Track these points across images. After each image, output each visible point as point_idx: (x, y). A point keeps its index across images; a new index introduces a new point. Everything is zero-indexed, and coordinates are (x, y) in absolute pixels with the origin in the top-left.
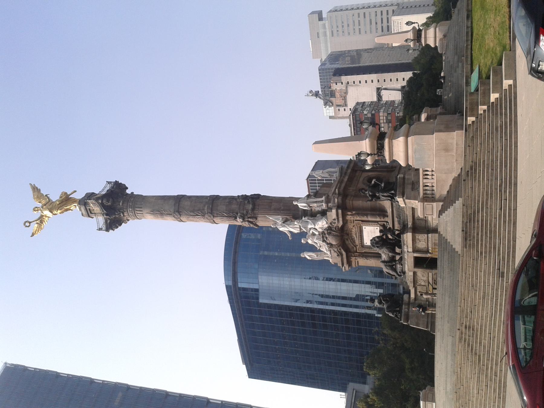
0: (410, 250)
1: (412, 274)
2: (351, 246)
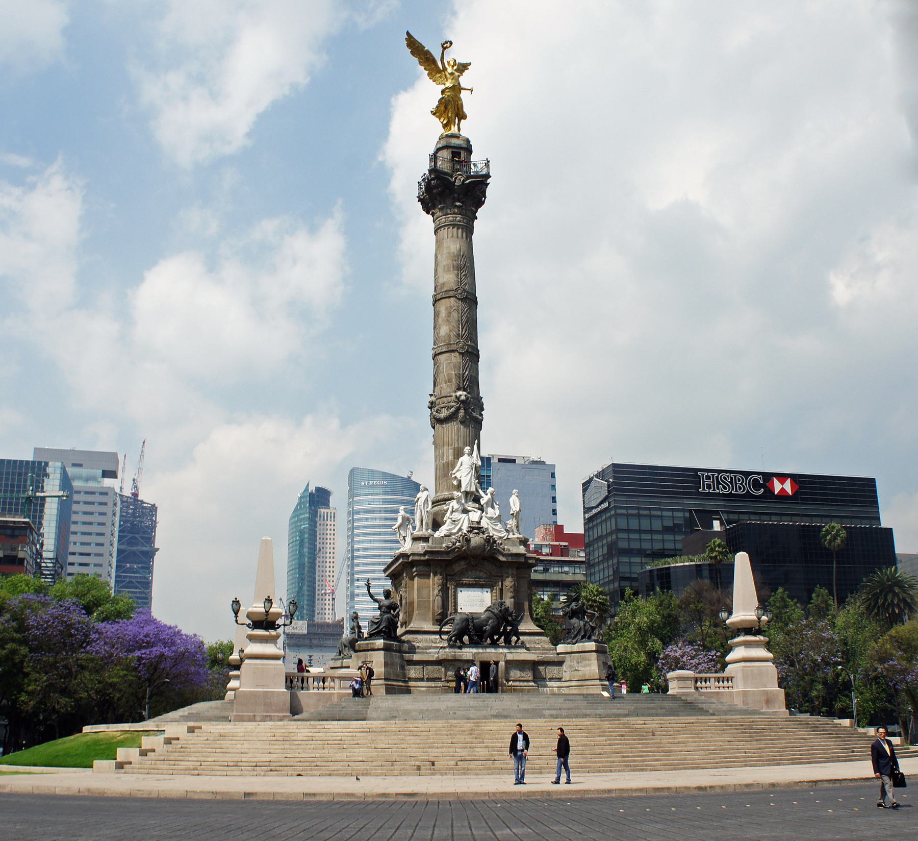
0: (510, 657)
1: (469, 657)
2: (457, 568)
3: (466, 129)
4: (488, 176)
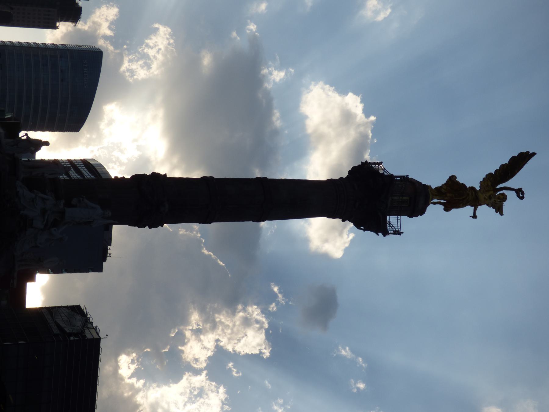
3: (435, 210)
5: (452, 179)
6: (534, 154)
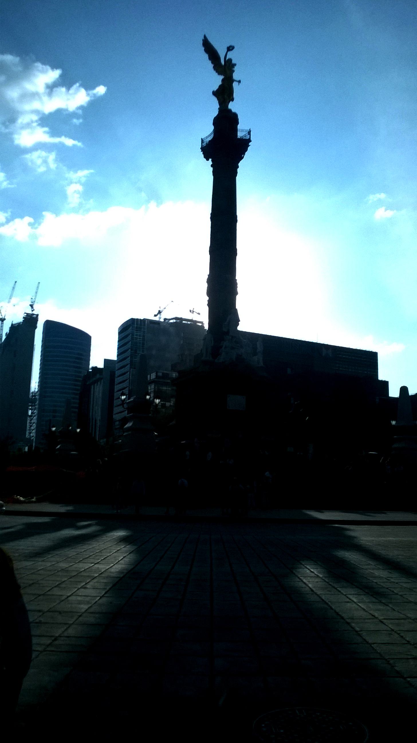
4: (249, 140)
5: (215, 93)
6: (205, 36)
